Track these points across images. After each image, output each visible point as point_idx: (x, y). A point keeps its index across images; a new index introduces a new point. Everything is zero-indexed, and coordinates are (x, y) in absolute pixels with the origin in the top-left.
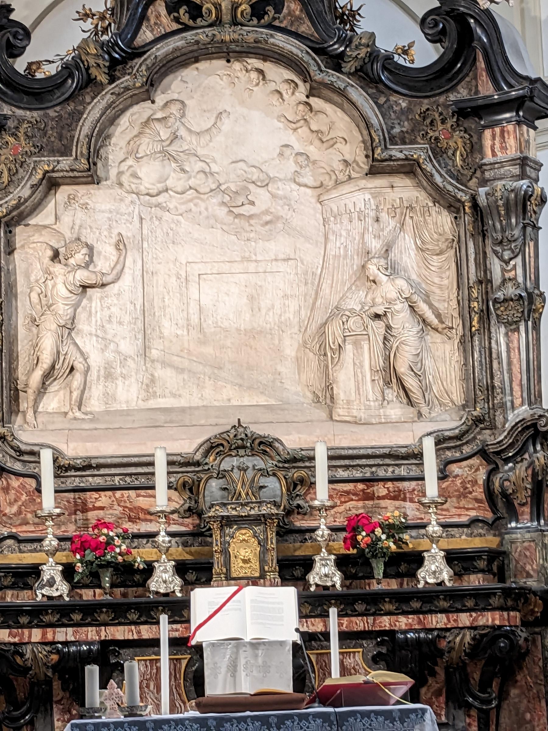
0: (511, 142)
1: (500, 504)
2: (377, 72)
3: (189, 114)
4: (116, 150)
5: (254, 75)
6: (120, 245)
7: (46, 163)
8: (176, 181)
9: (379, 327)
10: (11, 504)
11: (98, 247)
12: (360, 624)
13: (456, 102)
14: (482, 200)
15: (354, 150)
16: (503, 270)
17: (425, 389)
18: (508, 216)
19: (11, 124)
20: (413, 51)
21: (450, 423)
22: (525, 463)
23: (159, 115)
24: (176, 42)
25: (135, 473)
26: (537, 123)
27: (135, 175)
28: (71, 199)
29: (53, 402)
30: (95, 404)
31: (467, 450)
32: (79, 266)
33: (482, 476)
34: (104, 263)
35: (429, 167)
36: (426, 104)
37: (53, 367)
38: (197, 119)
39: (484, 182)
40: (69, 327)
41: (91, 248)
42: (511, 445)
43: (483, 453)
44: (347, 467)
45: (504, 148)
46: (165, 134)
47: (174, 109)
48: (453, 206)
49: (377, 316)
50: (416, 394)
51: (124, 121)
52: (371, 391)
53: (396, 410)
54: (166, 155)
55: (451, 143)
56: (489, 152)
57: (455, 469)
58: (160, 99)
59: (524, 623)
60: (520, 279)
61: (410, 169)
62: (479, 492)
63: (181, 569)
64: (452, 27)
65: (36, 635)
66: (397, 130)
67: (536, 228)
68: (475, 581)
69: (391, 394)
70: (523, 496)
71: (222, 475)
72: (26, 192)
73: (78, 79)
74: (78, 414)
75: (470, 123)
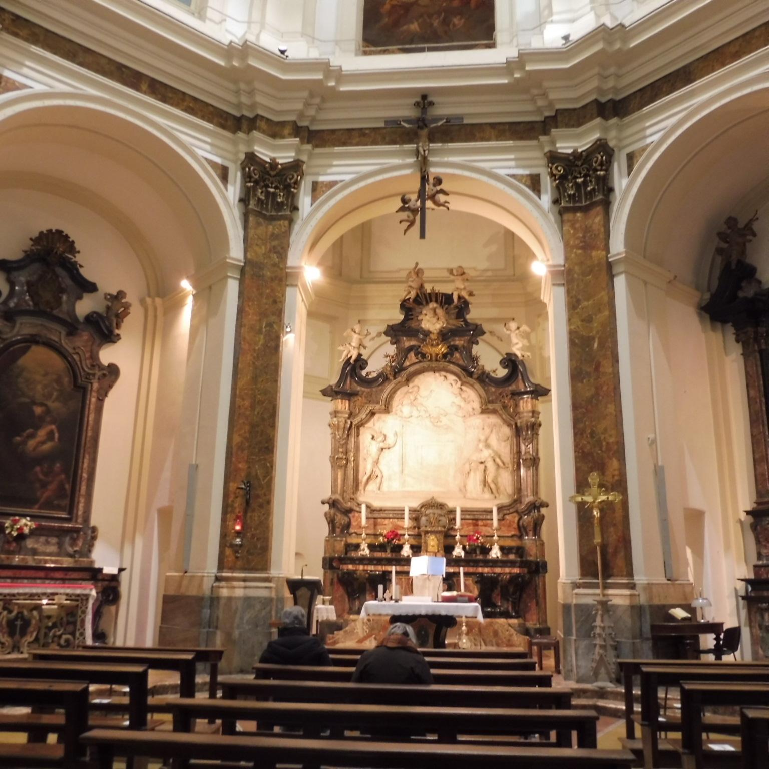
0: (529, 405)
1: (522, 529)
2: (484, 379)
3: (420, 390)
4: (395, 402)
5: (443, 378)
6: (396, 434)
7: (371, 407)
8: (415, 413)
9: (482, 466)
10: (355, 521)
11: (388, 435)
12: (471, 570)
13: (511, 391)
14: (519, 424)
15: (476, 404)
16: (525, 449)
17: (498, 489)
18: (527, 431)
19: (360, 393)
20: (497, 372)
21: (505, 500)
22: (531, 517)
23: (410, 390)
24: (417, 367)
25: (398, 513)
26: (539, 398)
27: (401, 411)
28: (379, 418)
29: (372, 486)
30: (385, 487)
31: (511, 510)
32: (381, 442)
33: (516, 519)
34: (390, 440)
35: (500, 412)
36: (501, 390)
37: (371, 475)
38: (423, 392)
39: (520, 418)
40: (377, 462)
41: (385, 436)
42: (526, 510)
43: (517, 511)
44: (469, 515)
45: (526, 406)
46: (412, 397)
47: (415, 389)
48: (509, 425)
49: (482, 463)
50: (494, 490)
51: (398, 392)
52: (479, 487)
53: (487, 495)
54: (412, 404)
55: (509, 404)
56: (522, 408)
57: (507, 517)
58: (411, 385)
59: (529, 572)
60: (531, 452)
61: (494, 411)
62: (515, 525)
63: (412, 547)
64: (510, 365)
65: (361, 567)
66: (490, 398)
67: (537, 434)
68: (512, 557)
69: (486, 489)
70: (531, 527)
71: (426, 515)
72: (364, 416)
73: (383, 378)
74: (379, 492)
75: (516, 397)
